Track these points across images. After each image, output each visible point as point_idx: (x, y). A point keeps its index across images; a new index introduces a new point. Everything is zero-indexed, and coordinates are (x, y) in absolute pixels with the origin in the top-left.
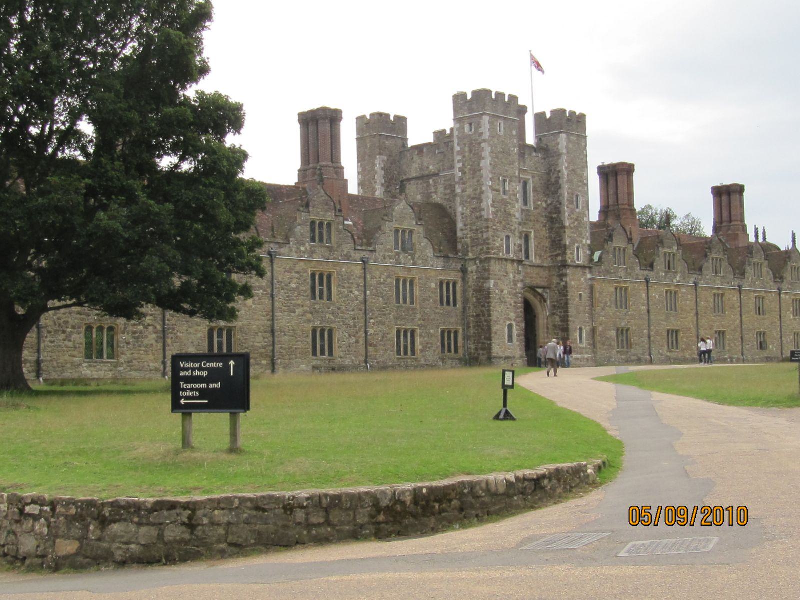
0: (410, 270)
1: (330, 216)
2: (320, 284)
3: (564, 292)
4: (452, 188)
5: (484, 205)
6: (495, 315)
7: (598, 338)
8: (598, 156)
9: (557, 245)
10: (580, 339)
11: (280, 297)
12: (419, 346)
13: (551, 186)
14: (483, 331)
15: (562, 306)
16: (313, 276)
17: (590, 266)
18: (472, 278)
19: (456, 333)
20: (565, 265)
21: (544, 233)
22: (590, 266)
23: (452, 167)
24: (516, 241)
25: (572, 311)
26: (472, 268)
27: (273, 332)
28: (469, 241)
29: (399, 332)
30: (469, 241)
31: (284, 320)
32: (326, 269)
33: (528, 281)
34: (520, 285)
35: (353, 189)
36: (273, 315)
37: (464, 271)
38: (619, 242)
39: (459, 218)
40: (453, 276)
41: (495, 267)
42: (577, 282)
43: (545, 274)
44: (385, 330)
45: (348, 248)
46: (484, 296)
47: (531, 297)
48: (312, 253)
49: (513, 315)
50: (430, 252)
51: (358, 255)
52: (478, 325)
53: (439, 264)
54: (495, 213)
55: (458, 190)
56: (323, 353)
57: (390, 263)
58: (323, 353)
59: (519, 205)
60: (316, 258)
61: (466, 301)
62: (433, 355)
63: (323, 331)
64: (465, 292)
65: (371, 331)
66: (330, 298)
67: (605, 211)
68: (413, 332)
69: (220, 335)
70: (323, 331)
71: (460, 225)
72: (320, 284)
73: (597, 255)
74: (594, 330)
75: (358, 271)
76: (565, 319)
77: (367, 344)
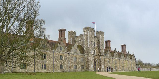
0: (76, 55)
1: (63, 46)
2: (61, 57)
3: (100, 60)
4: (83, 43)
5: (88, 45)
6: (90, 63)
7: (105, 67)
8: (106, 39)
9: (99, 52)
10: (103, 67)
11: (54, 59)
12: (77, 68)
13: (98, 43)
14: (88, 65)
15: (100, 62)
16: (60, 56)
17: (104, 56)
18: (86, 57)
19: (83, 66)
20: (101, 55)
21: (97, 50)
22: (104, 56)
23: (83, 39)
24: (93, 51)
25: (101, 63)
26: (86, 55)
27: (53, 65)
28: (86, 51)
29: (74, 65)
30: (86, 51)
31: (55, 63)
32: (62, 55)
33: (95, 58)
34: (94, 58)
35: (67, 42)
36: (53, 62)
37: (85, 56)
38: (108, 52)
39: (84, 47)
40: (83, 57)
41: (90, 55)
42: (102, 58)
43: (97, 57)
44: (72, 65)
45: (66, 51)
46: (88, 60)
47: (95, 60)
48: (60, 52)
49: (92, 63)
50: (79, 52)
51: (68, 53)
52: (87, 64)
53: (81, 54)
54: (90, 47)
55: (84, 43)
56: (62, 68)
57: (73, 54)
58: (62, 68)
59: (94, 46)
60: (61, 53)
61: (85, 61)
62: (80, 69)
63: (62, 65)
64: (85, 59)
65: (70, 65)
66: (63, 59)
67: (106, 48)
68: (76, 65)
69: (44, 65)
70: (62, 65)
71: (84, 48)
72: (61, 57)
73: (105, 54)
74: (105, 66)
75: (68, 55)
76: (101, 64)
77: (69, 67)
